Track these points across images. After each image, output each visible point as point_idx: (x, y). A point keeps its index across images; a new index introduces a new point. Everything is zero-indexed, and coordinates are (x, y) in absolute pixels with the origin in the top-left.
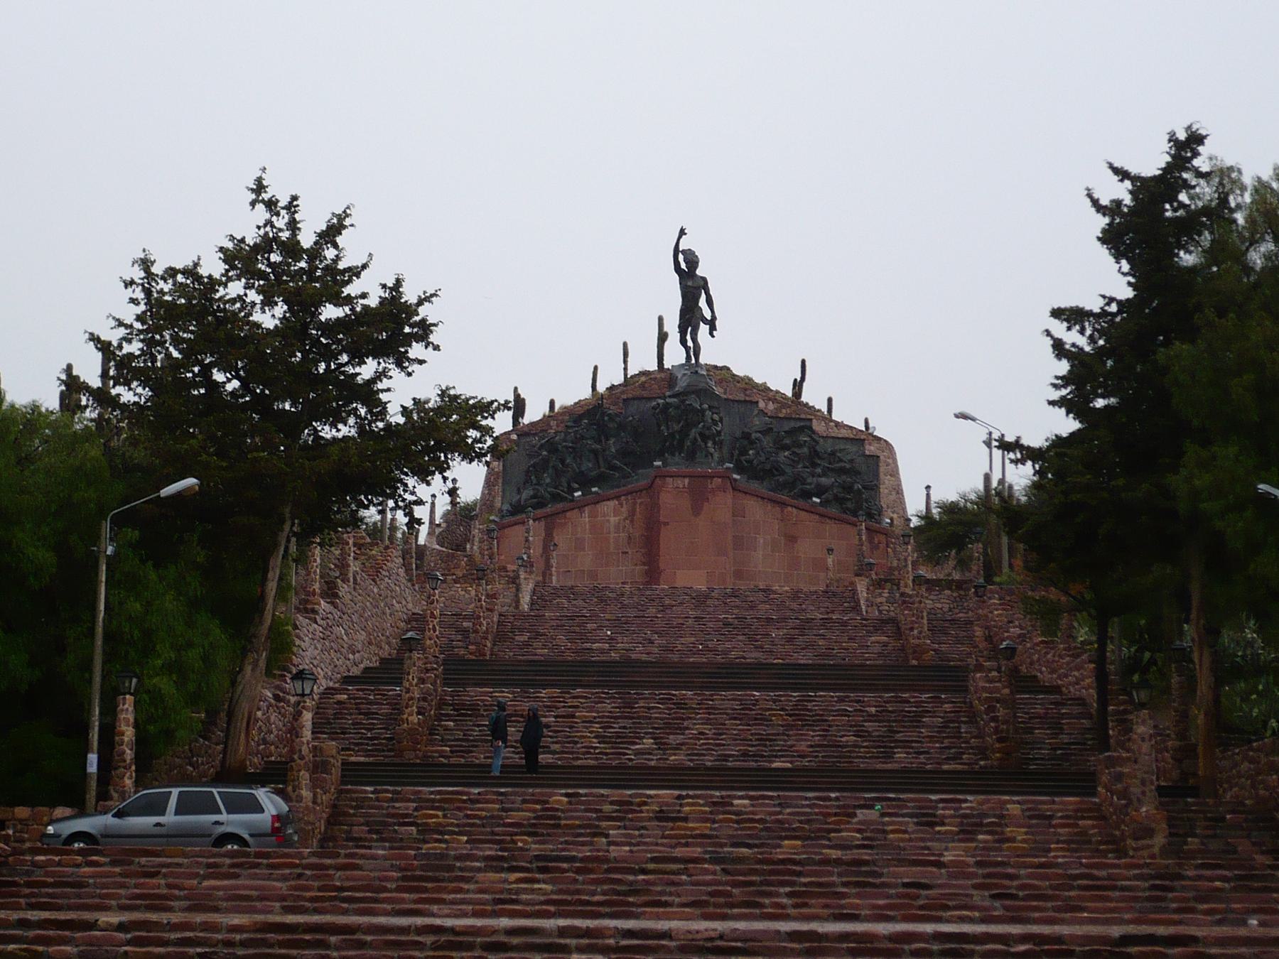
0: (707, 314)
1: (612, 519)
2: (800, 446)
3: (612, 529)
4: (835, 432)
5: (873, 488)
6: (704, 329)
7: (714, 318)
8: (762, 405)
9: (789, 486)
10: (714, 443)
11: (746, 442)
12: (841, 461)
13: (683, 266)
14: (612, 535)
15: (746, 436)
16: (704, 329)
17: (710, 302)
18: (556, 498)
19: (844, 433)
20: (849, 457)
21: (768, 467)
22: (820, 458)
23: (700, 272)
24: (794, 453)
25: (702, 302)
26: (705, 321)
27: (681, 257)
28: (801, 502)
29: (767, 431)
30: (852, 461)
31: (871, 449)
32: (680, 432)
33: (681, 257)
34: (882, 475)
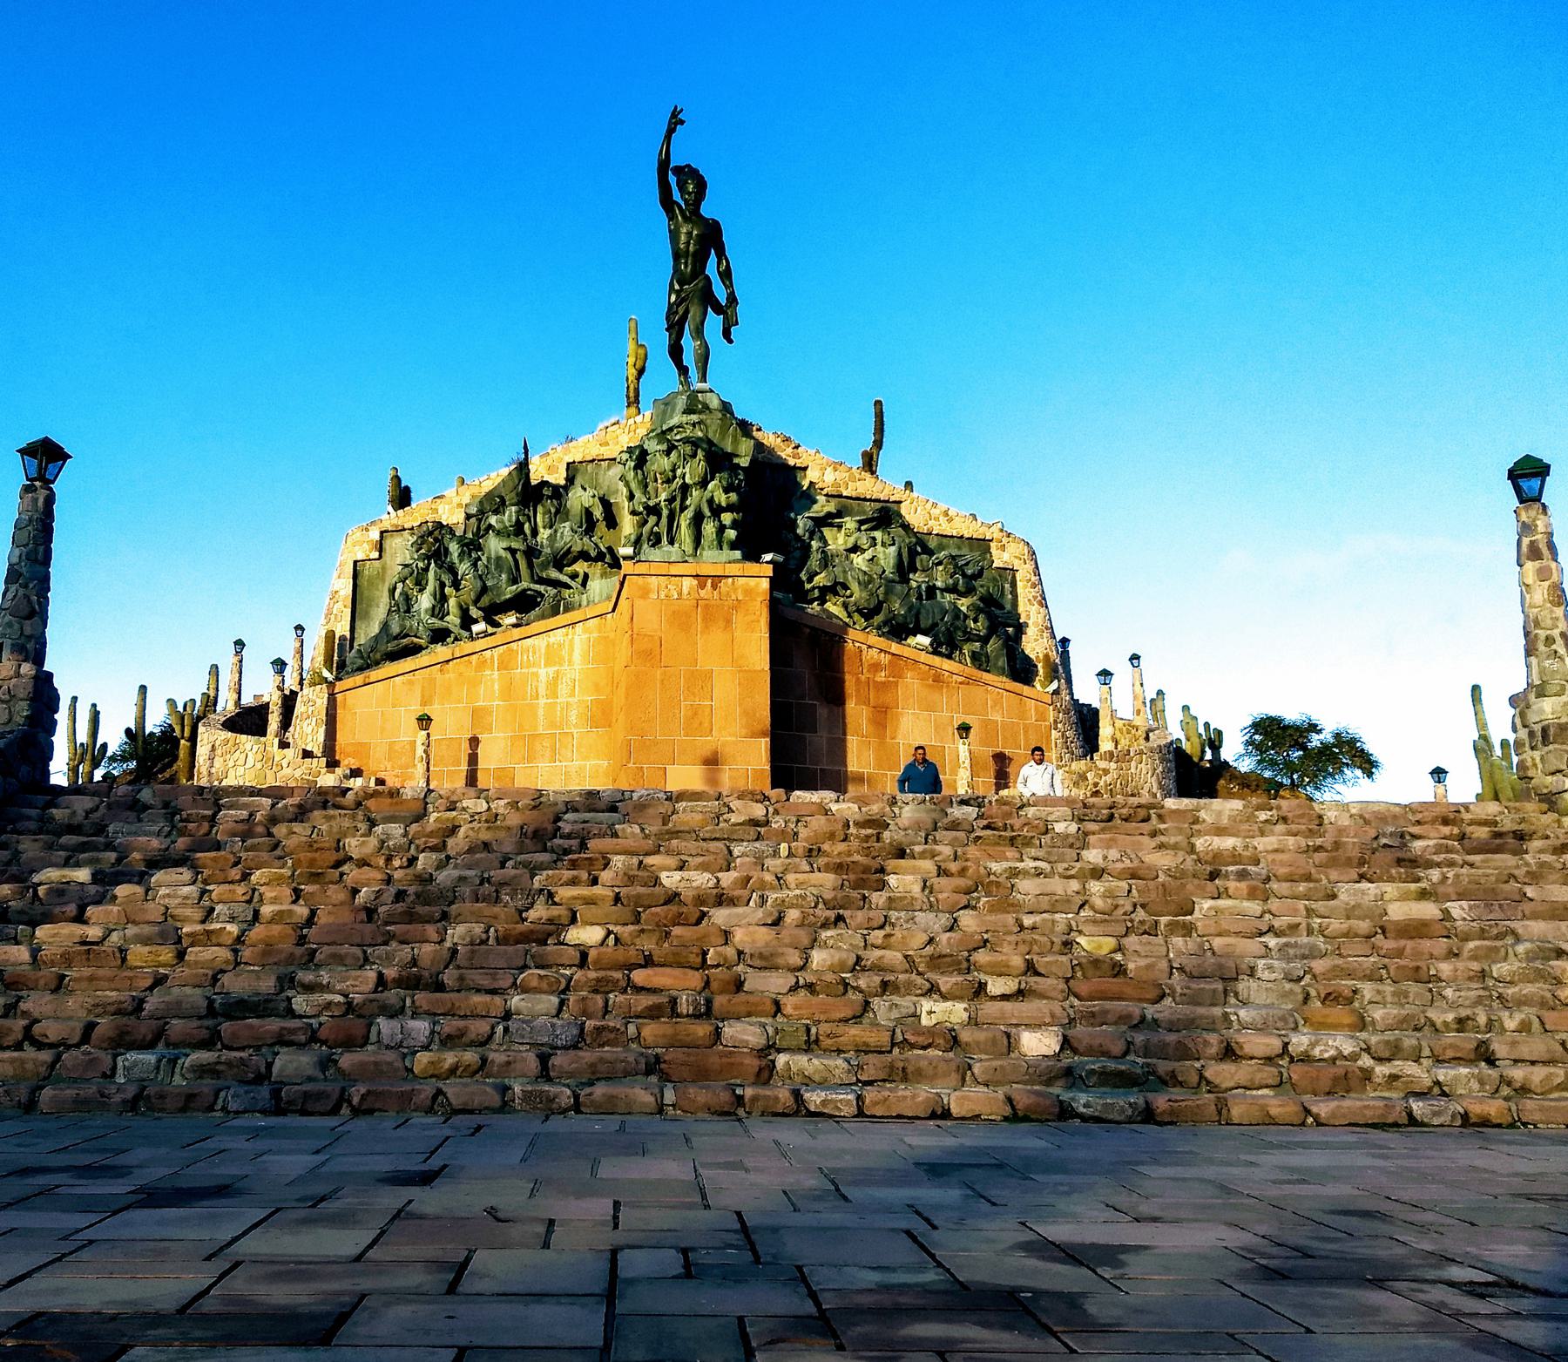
0: (720, 293)
1: (542, 672)
3: (542, 691)
6: (714, 322)
7: (732, 300)
13: (677, 196)
14: (542, 701)
16: (714, 322)
17: (726, 275)
18: (440, 636)
23: (707, 210)
25: (711, 268)
26: (719, 310)
27: (672, 179)
28: (895, 647)
32: (671, 500)
33: (672, 179)
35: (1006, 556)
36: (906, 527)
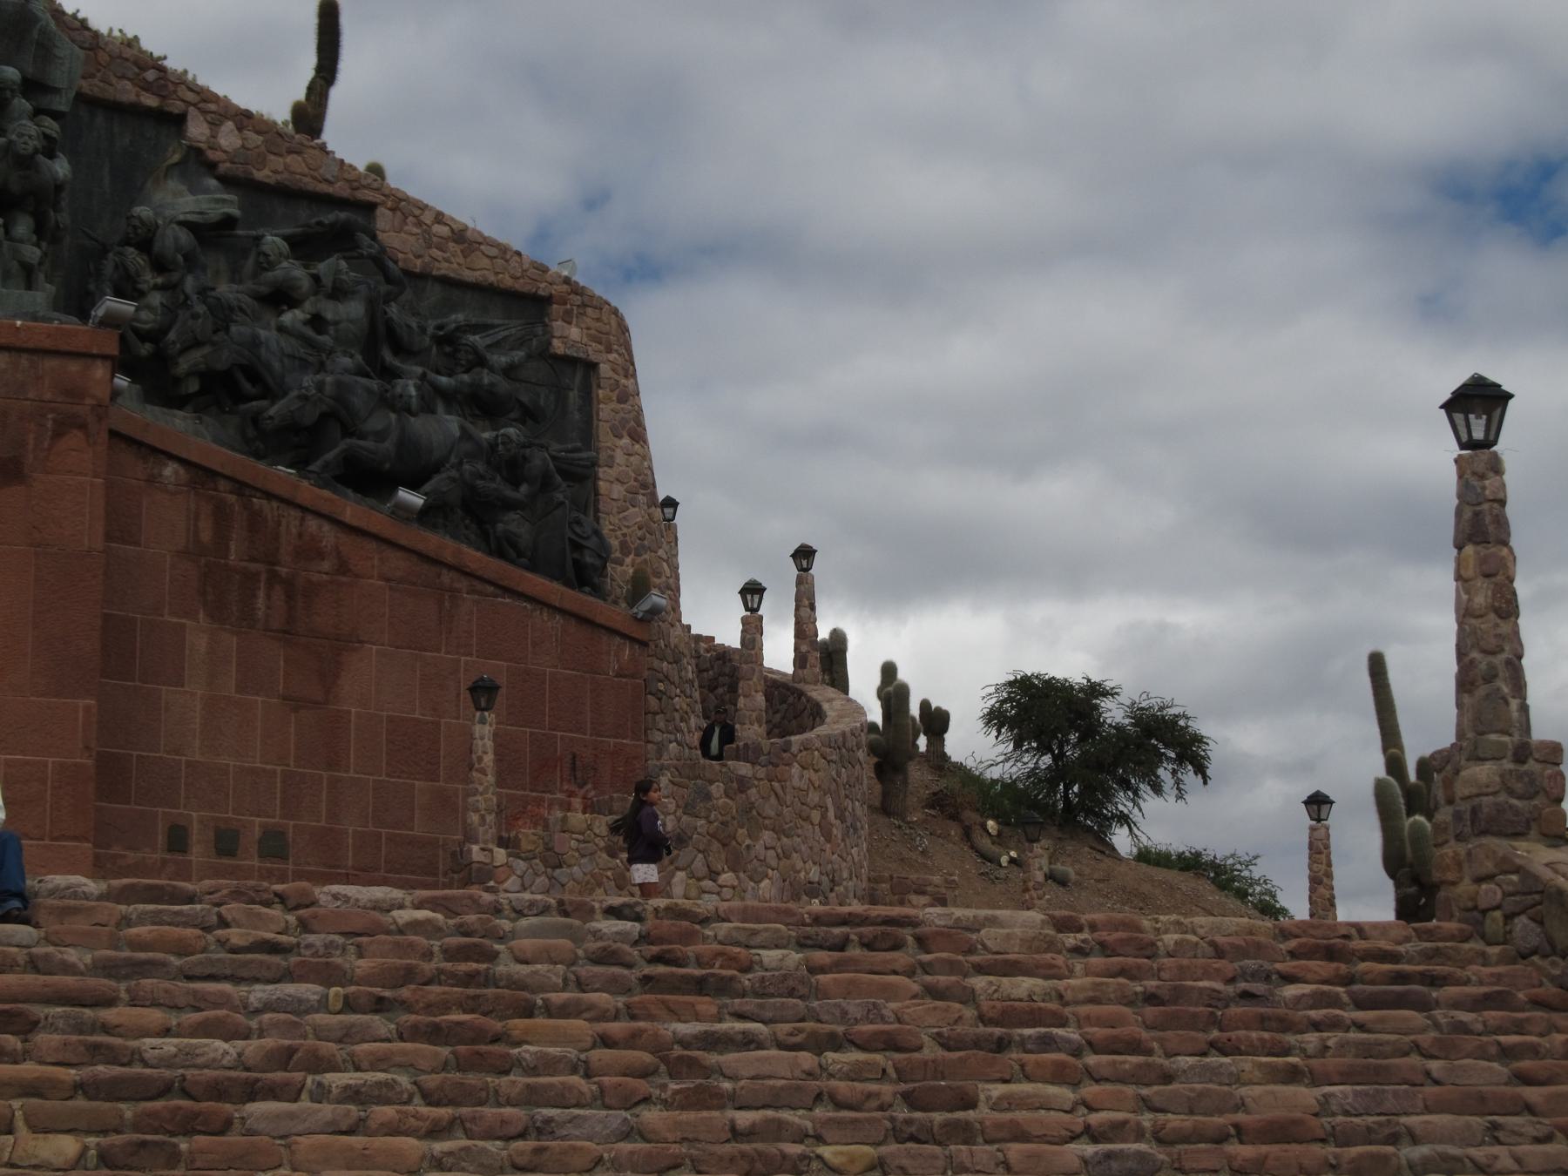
2: (338, 293)
4: (451, 264)
5: (581, 475)
8: (197, 129)
9: (297, 442)
10: (39, 230)
11: (133, 257)
12: (480, 361)
15: (145, 240)
19: (480, 270)
20: (500, 359)
21: (224, 360)
22: (401, 349)
24: (317, 321)
28: (352, 509)
29: (211, 233)
30: (509, 371)
31: (569, 336)
34: (603, 431)
35: (574, 333)
36: (380, 261)
